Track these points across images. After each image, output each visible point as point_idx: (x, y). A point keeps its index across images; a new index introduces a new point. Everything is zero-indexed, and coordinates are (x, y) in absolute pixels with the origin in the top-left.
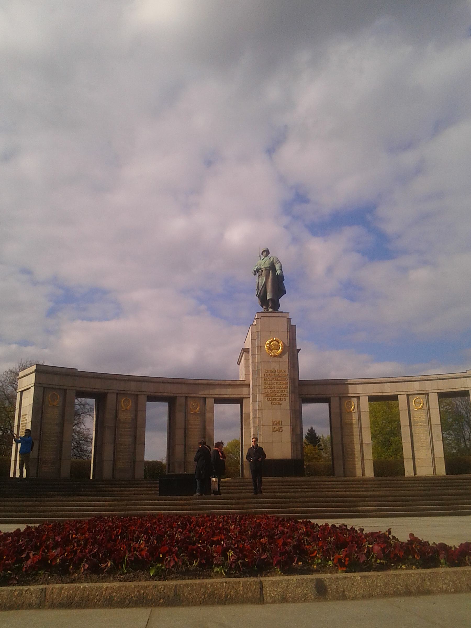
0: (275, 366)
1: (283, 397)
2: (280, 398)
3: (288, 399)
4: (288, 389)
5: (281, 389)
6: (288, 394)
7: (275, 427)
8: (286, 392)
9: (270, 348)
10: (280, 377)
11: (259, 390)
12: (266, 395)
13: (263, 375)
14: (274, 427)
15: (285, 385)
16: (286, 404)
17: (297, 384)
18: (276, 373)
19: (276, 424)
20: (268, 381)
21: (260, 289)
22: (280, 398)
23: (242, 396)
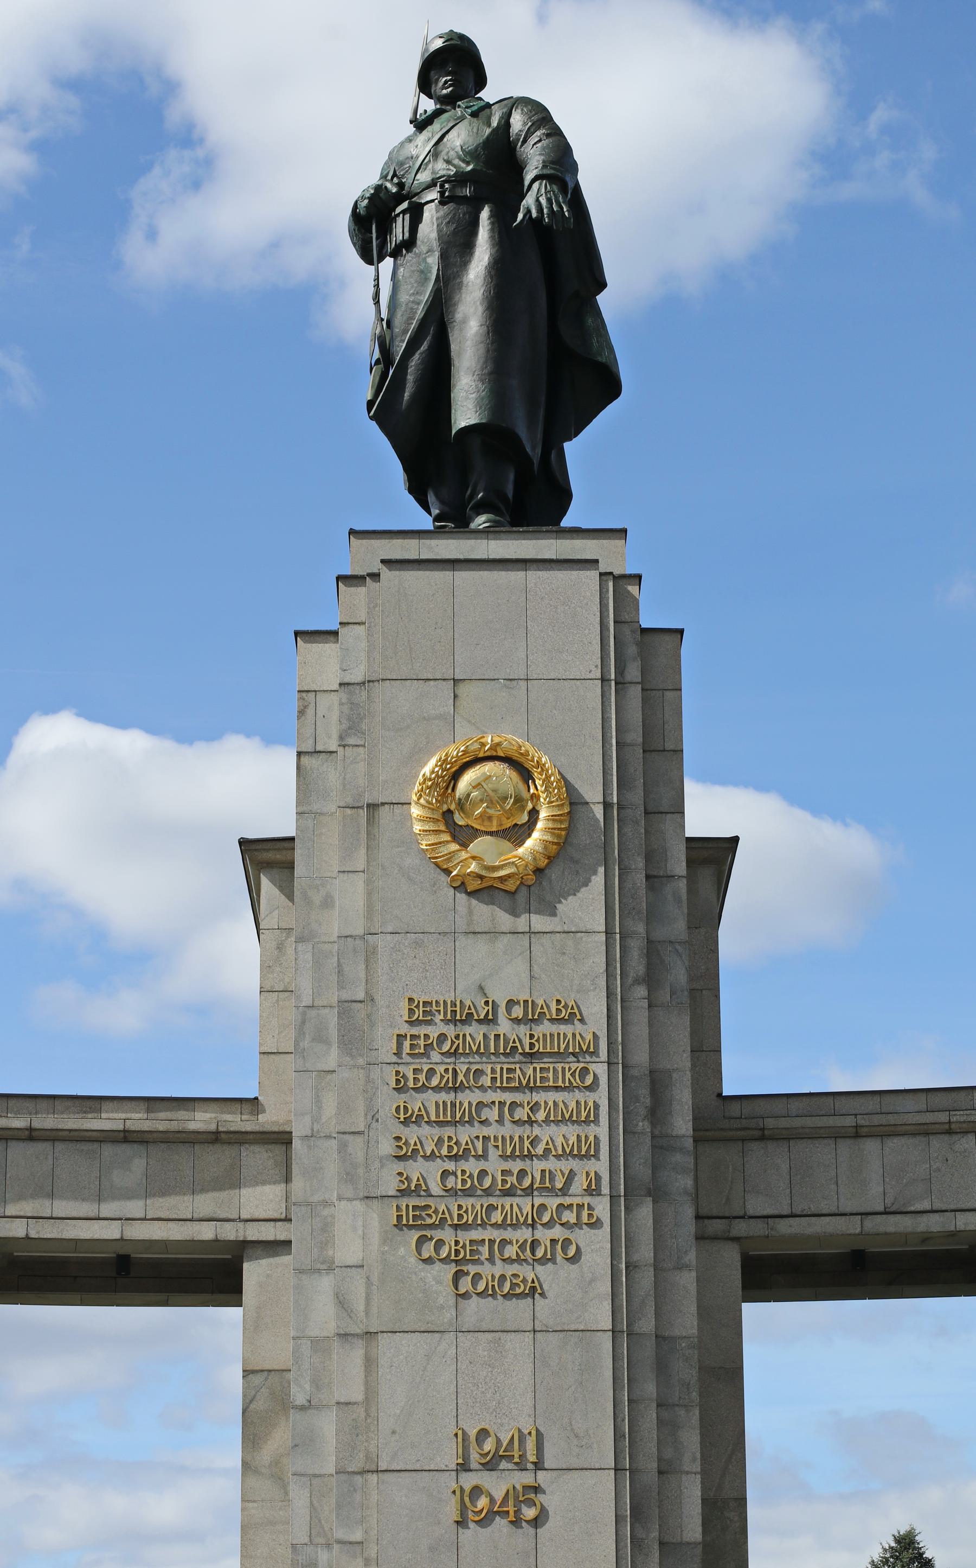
0: (499, 965)
1: (557, 1232)
2: (525, 1234)
3: (596, 1246)
4: (602, 1166)
5: (538, 1165)
6: (602, 1208)
7: (484, 1479)
8: (580, 1184)
9: (453, 824)
10: (531, 1056)
11: (349, 1177)
12: (415, 1217)
13: (387, 1049)
14: (468, 1481)
15: (572, 1132)
16: (582, 1289)
17: (682, 1124)
18: (504, 1026)
19: (490, 1465)
20: (431, 1099)
21: (400, 348)
22: (525, 1234)
23: (230, 1232)
